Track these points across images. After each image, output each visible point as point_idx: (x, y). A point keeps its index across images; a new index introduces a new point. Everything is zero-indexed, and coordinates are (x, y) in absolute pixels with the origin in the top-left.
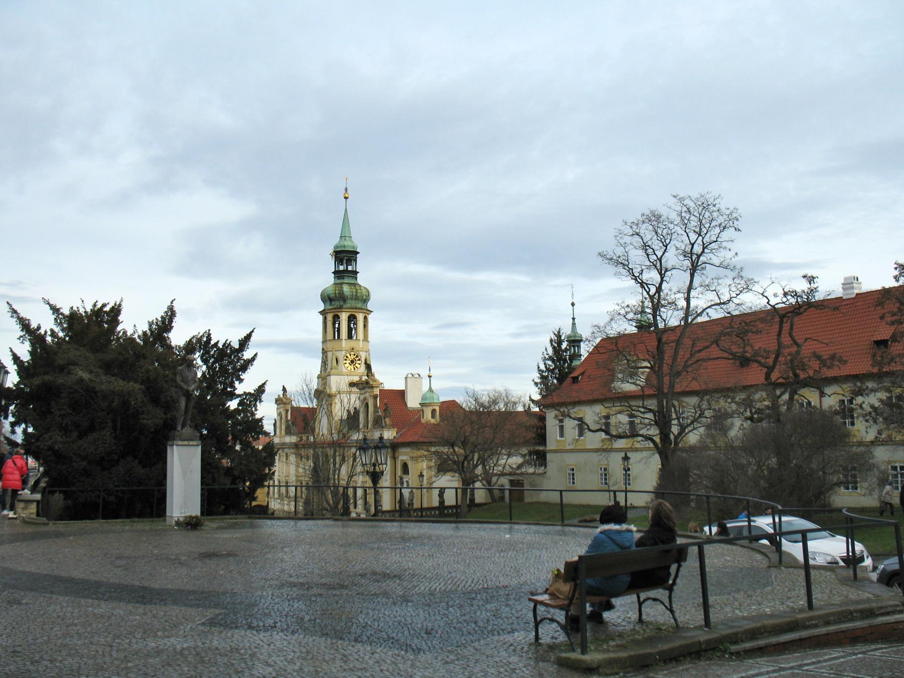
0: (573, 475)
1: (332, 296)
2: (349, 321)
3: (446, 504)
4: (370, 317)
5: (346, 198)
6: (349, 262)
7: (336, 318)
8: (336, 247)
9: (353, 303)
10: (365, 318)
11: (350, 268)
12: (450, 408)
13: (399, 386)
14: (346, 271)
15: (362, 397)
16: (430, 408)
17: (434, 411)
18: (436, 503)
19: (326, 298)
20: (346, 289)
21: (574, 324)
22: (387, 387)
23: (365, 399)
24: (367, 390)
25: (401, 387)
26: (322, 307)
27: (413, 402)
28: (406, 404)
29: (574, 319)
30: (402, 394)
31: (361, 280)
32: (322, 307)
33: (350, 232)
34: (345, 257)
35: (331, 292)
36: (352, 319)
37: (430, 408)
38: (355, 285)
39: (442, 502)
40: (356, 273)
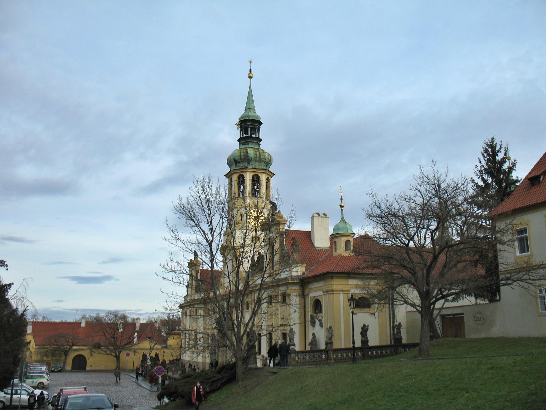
1: (238, 158)
2: (253, 180)
3: (371, 343)
4: (272, 180)
5: (250, 78)
7: (241, 180)
8: (242, 117)
9: (257, 165)
10: (268, 179)
16: (344, 239)
17: (348, 242)
18: (358, 344)
20: (250, 152)
28: (312, 244)
30: (308, 235)
31: (263, 146)
33: (254, 106)
34: (249, 127)
36: (256, 180)
37: (344, 239)
38: (258, 149)
39: (365, 342)
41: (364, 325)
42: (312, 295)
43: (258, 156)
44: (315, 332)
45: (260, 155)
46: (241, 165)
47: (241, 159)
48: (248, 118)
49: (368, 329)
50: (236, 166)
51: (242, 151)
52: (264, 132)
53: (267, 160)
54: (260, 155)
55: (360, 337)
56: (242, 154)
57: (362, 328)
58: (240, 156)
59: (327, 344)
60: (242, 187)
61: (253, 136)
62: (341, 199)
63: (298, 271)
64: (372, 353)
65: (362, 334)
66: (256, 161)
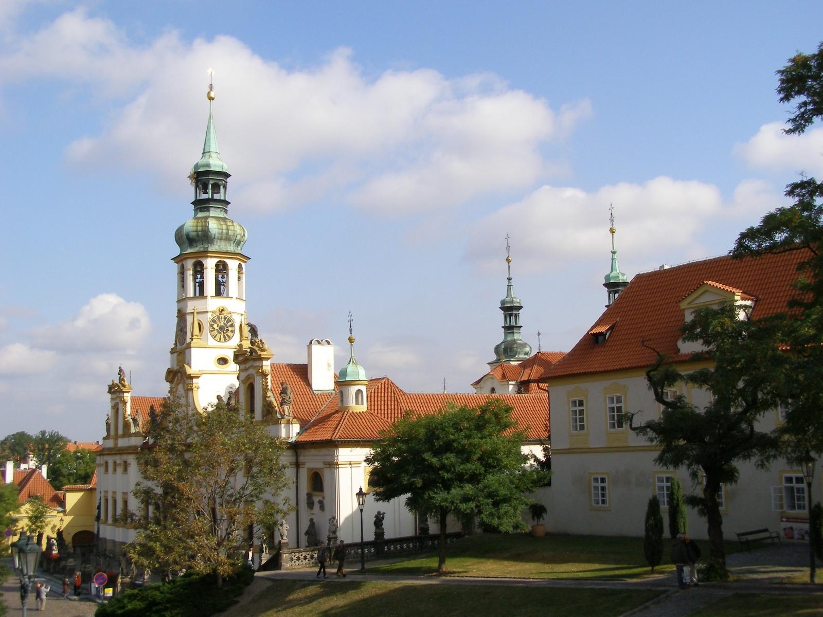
0: (603, 489)
1: (193, 234)
2: (218, 270)
6: (216, 187)
7: (199, 269)
10: (240, 266)
11: (220, 196)
14: (212, 200)
15: (244, 375)
18: (370, 536)
19: (184, 239)
20: (213, 226)
23: (249, 377)
26: (177, 251)
29: (509, 279)
32: (177, 251)
36: (221, 268)
39: (379, 533)
41: (379, 513)
42: (308, 465)
43: (225, 231)
44: (313, 517)
45: (228, 229)
47: (198, 235)
48: (207, 169)
49: (383, 518)
51: (200, 224)
53: (239, 237)
54: (228, 229)
55: (374, 528)
56: (200, 228)
57: (376, 517)
58: (197, 231)
59: (329, 539)
60: (199, 276)
61: (216, 196)
62: (351, 331)
64: (389, 549)
65: (375, 523)
66: (221, 239)
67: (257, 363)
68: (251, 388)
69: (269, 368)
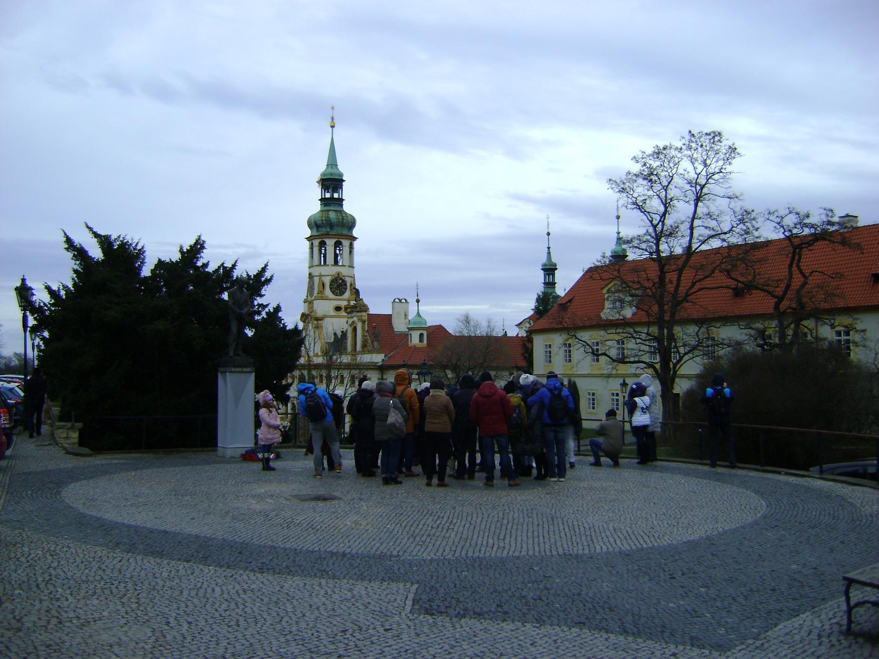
1: (319, 222)
4: (355, 243)
5: (333, 127)
7: (322, 244)
8: (323, 174)
12: (437, 333)
13: (387, 310)
14: (332, 198)
15: (350, 321)
17: (421, 335)
19: (313, 224)
20: (332, 215)
21: (549, 253)
22: (373, 311)
23: (353, 323)
24: (355, 314)
25: (388, 311)
26: (308, 233)
27: (399, 326)
29: (549, 248)
30: (387, 319)
31: (347, 207)
34: (332, 183)
35: (318, 219)
40: (340, 201)
46: (323, 230)
50: (318, 231)
52: (348, 192)
61: (336, 196)
63: (378, 358)
66: (338, 226)
67: (359, 314)
68: (355, 329)
69: (366, 318)
